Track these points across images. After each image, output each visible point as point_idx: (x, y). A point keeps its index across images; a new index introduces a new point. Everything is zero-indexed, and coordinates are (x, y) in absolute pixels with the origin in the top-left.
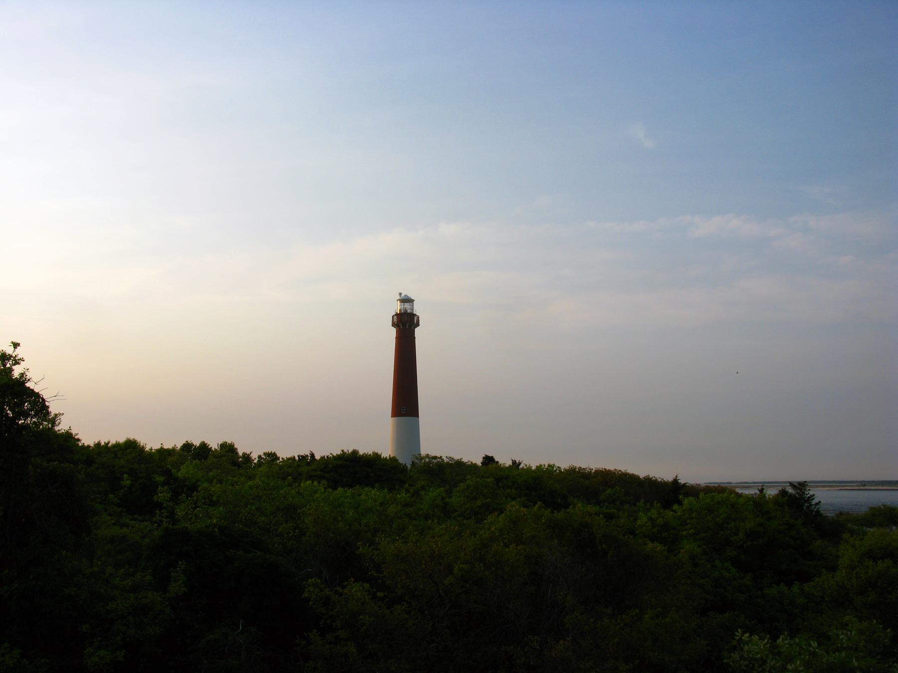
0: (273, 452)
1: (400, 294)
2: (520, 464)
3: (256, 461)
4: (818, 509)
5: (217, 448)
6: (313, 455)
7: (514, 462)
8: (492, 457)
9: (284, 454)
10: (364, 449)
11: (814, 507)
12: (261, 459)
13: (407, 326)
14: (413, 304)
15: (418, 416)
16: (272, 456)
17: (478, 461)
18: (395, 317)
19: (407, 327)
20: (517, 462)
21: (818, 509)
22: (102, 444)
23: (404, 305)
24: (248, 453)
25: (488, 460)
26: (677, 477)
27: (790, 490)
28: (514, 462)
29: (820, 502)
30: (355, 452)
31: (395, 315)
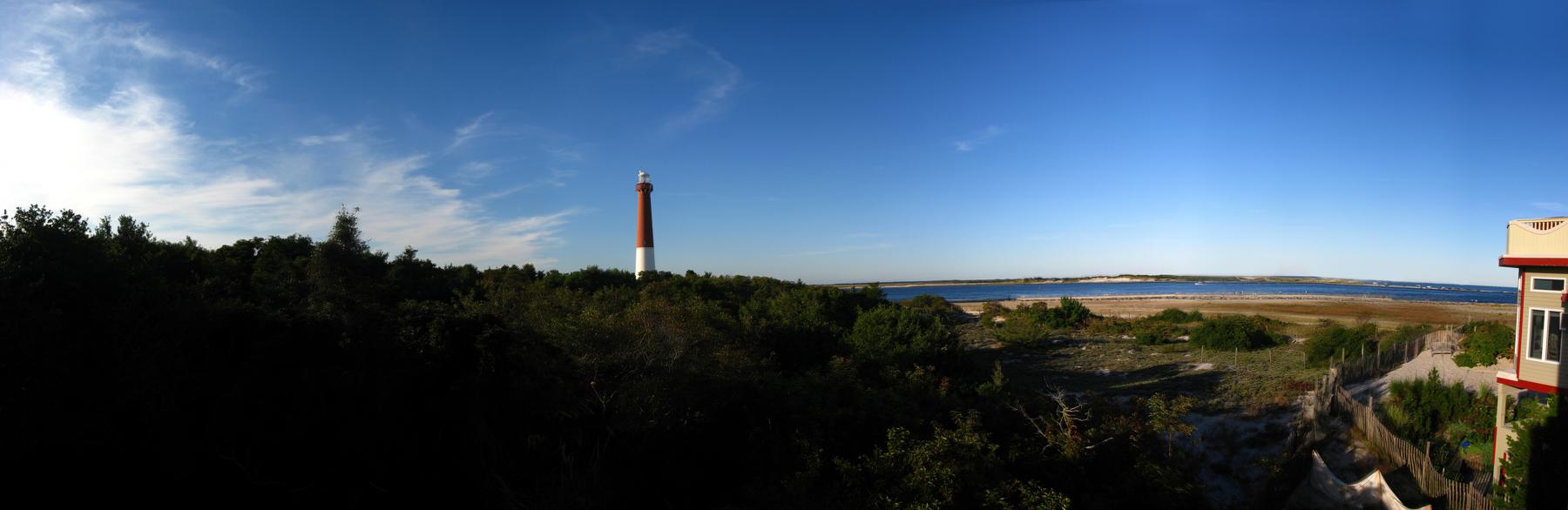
7: (707, 274)
15: (653, 246)
16: (555, 273)
17: (684, 274)
25: (690, 273)
28: (707, 274)
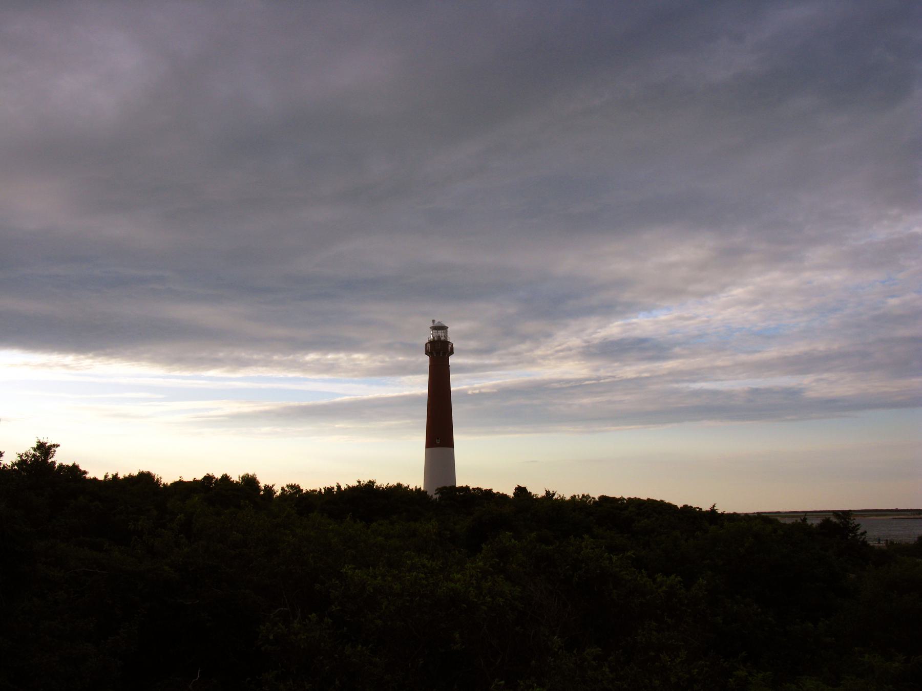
0: (296, 485)
1: (433, 321)
2: (554, 494)
3: (278, 494)
4: (865, 538)
5: (238, 480)
6: (339, 487)
7: (548, 493)
8: (525, 488)
9: (306, 487)
10: (384, 481)
11: (859, 537)
12: (284, 492)
13: (441, 353)
14: (447, 331)
16: (295, 488)
17: (510, 493)
18: (429, 345)
19: (441, 355)
20: (551, 492)
21: (865, 538)
22: (109, 477)
23: (437, 332)
24: (271, 485)
25: (521, 491)
26: (714, 506)
27: (834, 520)
28: (548, 493)
29: (865, 532)
30: (371, 483)
31: (429, 343)
